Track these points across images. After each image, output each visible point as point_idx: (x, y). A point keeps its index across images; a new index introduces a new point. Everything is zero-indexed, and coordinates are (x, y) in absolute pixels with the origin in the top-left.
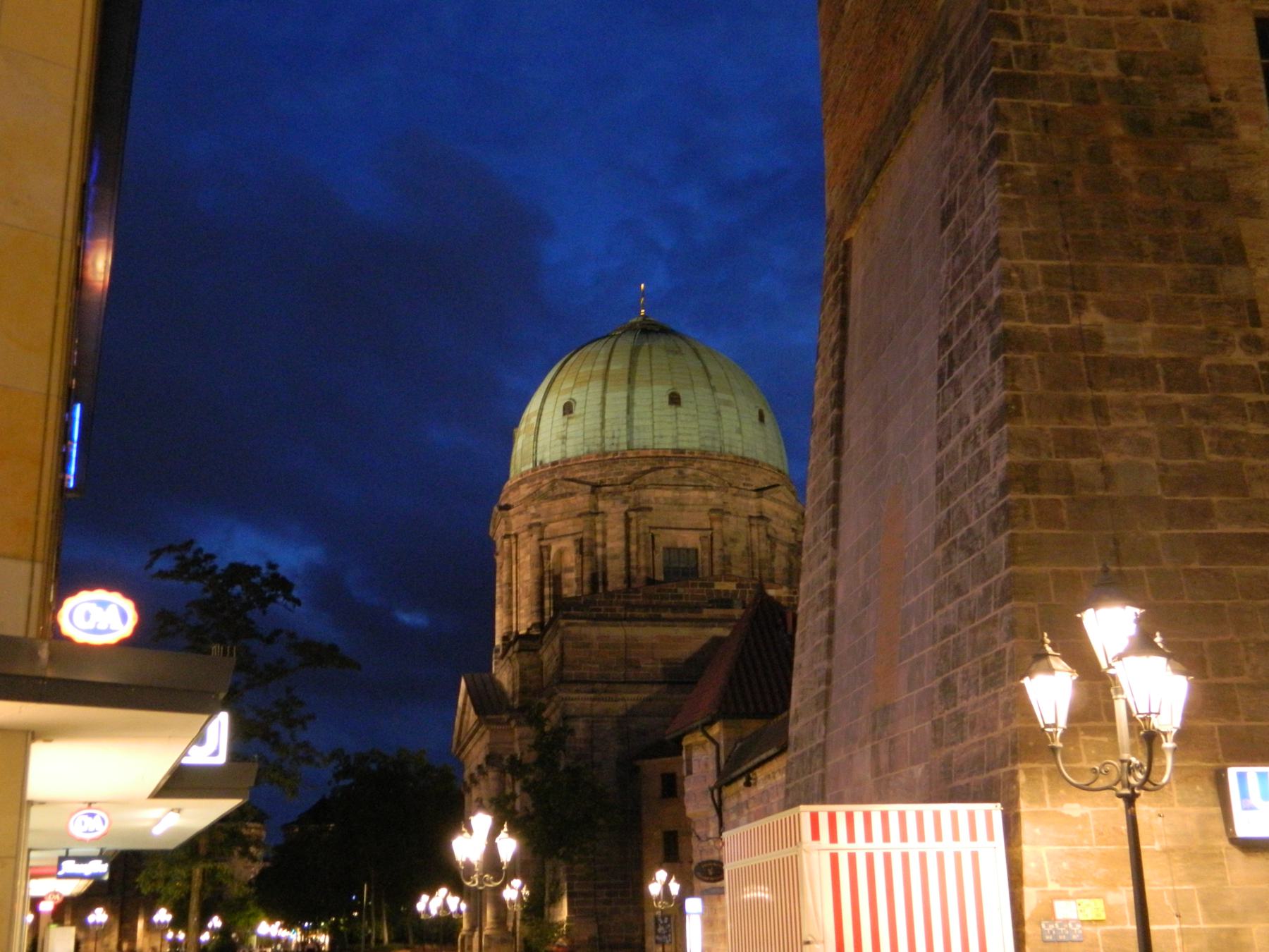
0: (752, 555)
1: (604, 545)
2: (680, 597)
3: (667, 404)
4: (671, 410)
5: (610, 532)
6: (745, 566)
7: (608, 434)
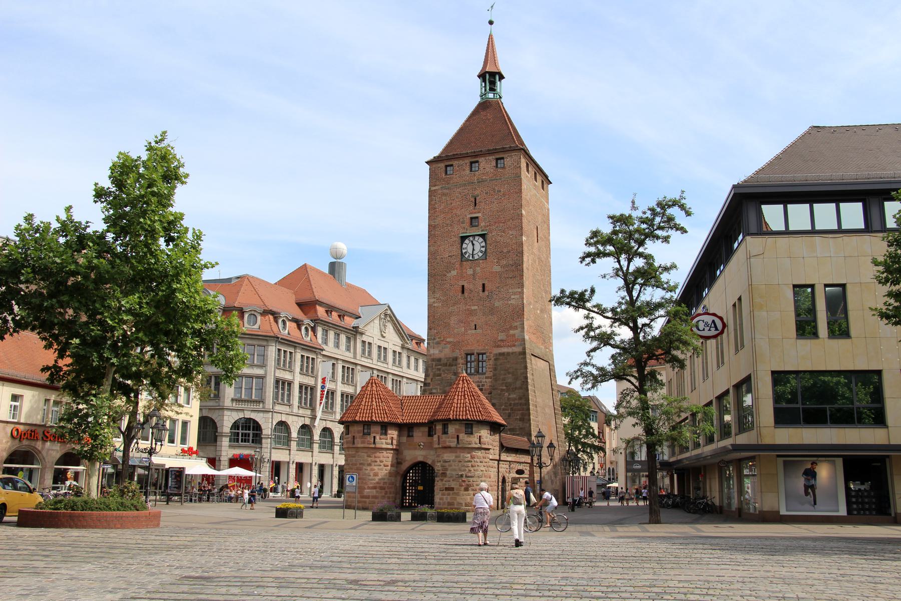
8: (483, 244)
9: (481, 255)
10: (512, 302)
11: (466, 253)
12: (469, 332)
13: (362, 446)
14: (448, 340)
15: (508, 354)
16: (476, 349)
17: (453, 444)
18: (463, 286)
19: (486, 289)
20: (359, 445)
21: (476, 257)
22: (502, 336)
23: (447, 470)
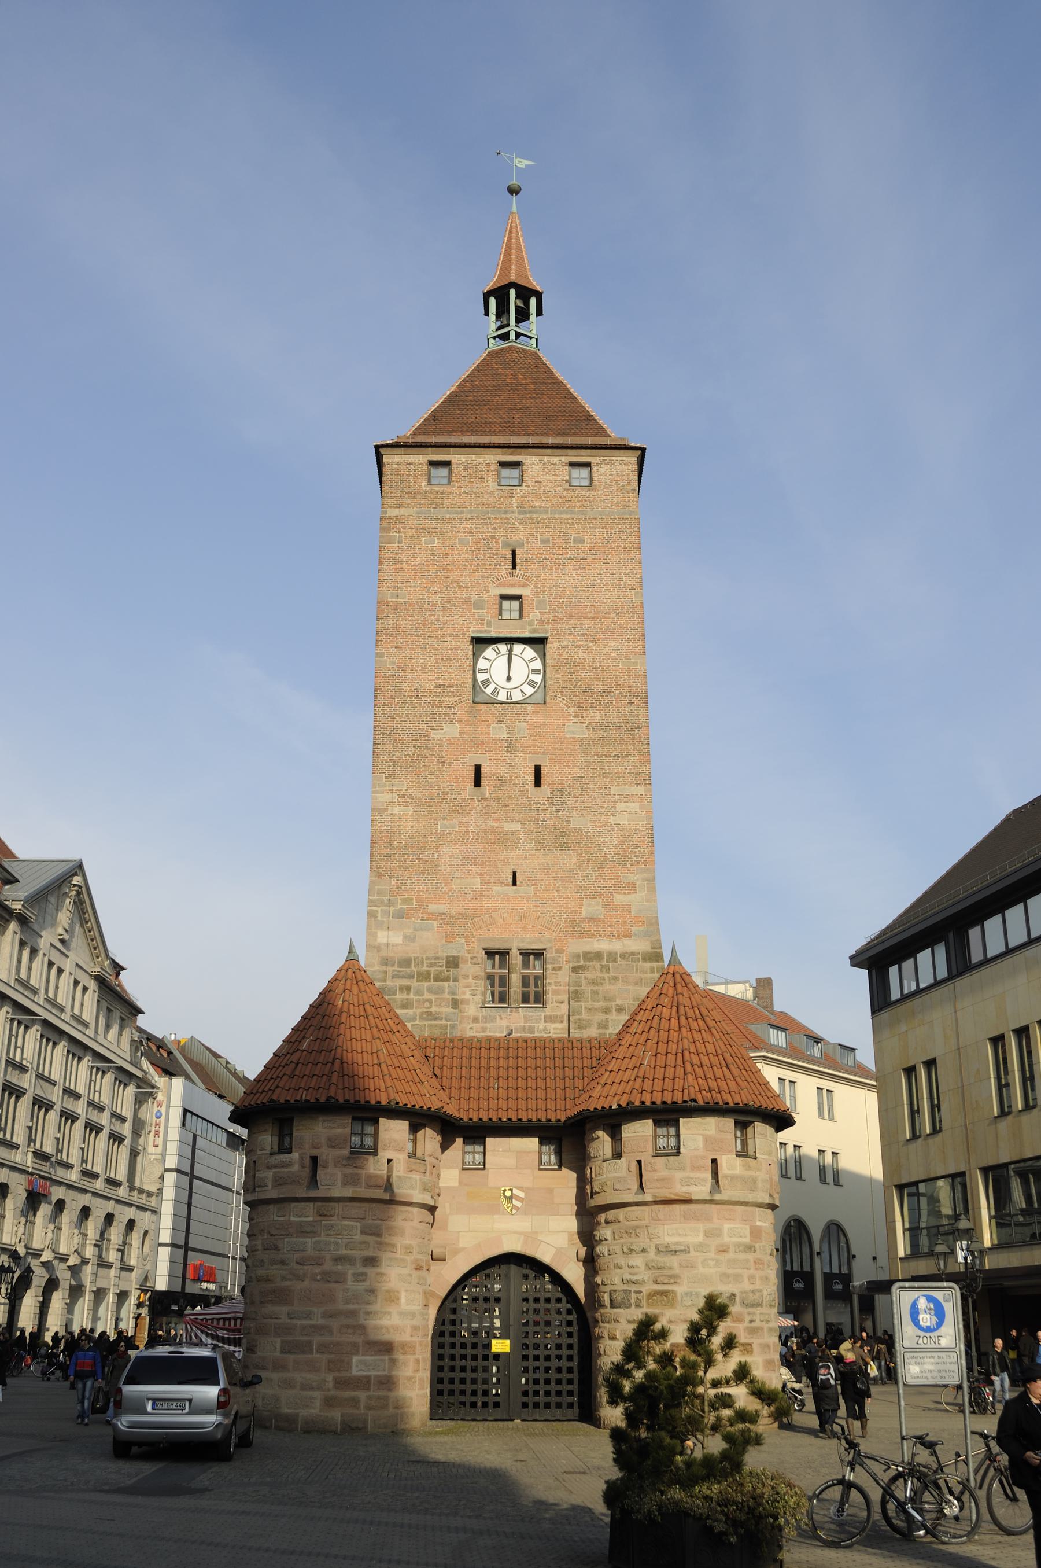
8: (538, 665)
9: (529, 690)
10: (623, 820)
11: (486, 683)
12: (496, 889)
13: (348, 1192)
14: (433, 908)
15: (612, 956)
16: (518, 939)
17: (701, 1189)
18: (478, 769)
19: (544, 779)
20: (337, 1192)
21: (517, 696)
22: (592, 908)
23: (674, 1279)
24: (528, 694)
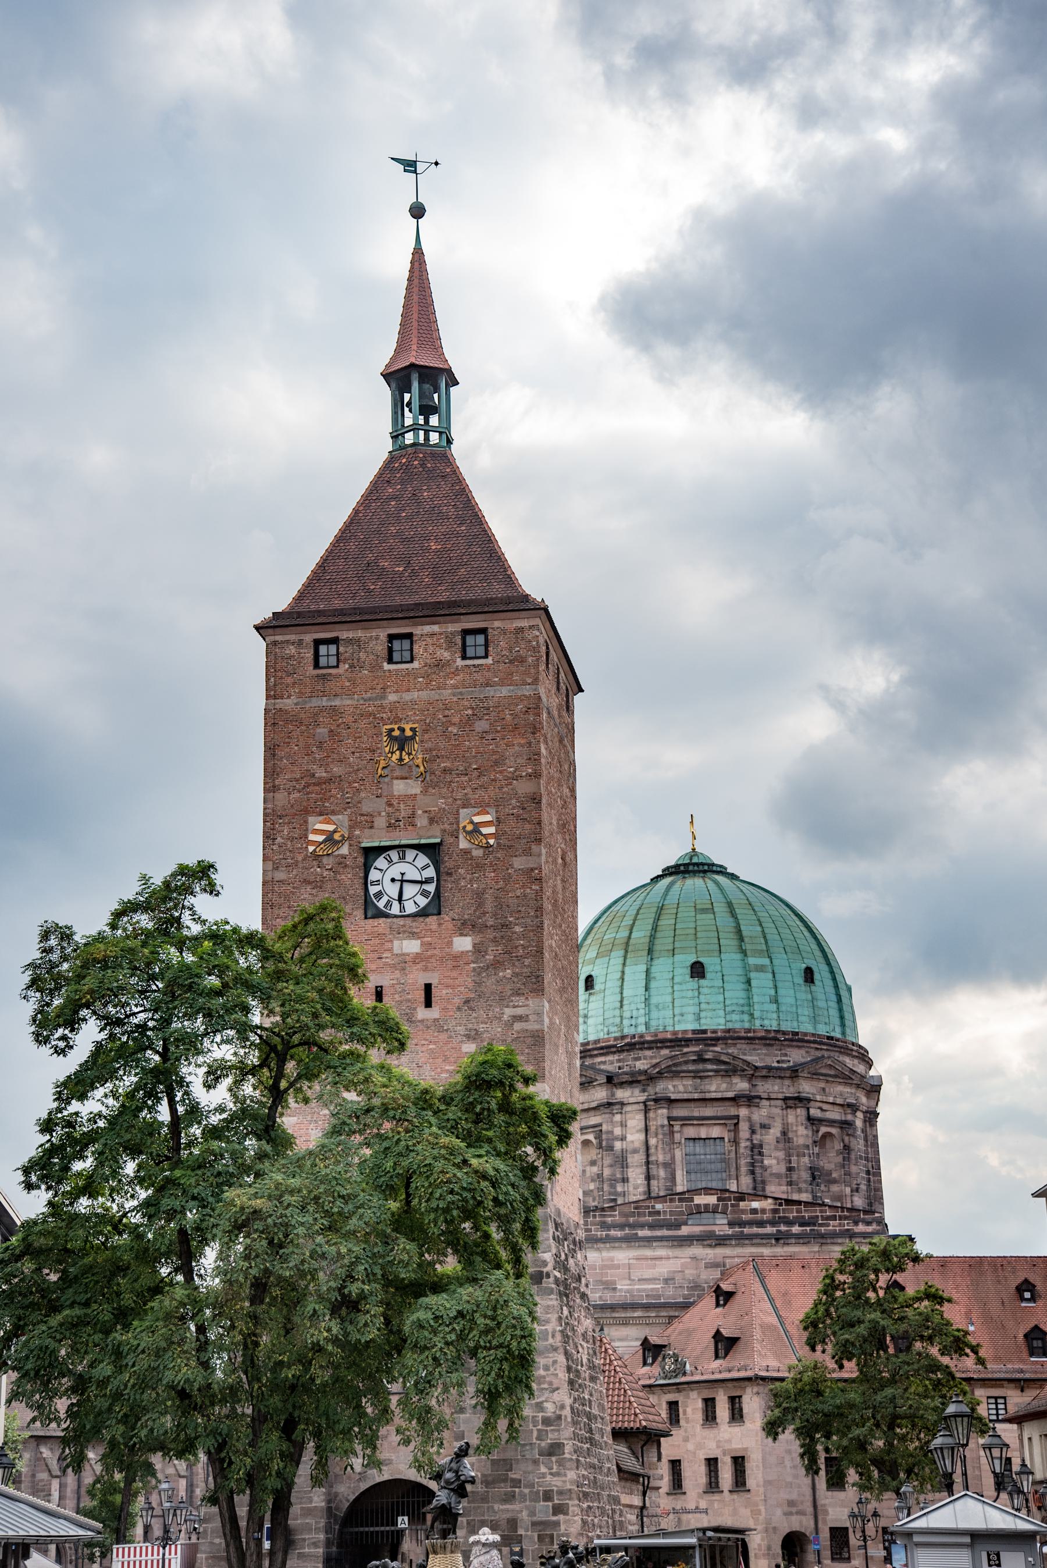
0: (789, 1140)
1: (623, 1139)
2: (658, 1213)
3: (688, 977)
4: (693, 984)
5: (630, 1123)
6: (781, 1154)
7: (627, 1014)
11: (379, 895)
24: (422, 905)
